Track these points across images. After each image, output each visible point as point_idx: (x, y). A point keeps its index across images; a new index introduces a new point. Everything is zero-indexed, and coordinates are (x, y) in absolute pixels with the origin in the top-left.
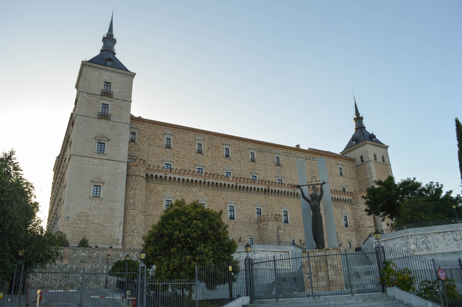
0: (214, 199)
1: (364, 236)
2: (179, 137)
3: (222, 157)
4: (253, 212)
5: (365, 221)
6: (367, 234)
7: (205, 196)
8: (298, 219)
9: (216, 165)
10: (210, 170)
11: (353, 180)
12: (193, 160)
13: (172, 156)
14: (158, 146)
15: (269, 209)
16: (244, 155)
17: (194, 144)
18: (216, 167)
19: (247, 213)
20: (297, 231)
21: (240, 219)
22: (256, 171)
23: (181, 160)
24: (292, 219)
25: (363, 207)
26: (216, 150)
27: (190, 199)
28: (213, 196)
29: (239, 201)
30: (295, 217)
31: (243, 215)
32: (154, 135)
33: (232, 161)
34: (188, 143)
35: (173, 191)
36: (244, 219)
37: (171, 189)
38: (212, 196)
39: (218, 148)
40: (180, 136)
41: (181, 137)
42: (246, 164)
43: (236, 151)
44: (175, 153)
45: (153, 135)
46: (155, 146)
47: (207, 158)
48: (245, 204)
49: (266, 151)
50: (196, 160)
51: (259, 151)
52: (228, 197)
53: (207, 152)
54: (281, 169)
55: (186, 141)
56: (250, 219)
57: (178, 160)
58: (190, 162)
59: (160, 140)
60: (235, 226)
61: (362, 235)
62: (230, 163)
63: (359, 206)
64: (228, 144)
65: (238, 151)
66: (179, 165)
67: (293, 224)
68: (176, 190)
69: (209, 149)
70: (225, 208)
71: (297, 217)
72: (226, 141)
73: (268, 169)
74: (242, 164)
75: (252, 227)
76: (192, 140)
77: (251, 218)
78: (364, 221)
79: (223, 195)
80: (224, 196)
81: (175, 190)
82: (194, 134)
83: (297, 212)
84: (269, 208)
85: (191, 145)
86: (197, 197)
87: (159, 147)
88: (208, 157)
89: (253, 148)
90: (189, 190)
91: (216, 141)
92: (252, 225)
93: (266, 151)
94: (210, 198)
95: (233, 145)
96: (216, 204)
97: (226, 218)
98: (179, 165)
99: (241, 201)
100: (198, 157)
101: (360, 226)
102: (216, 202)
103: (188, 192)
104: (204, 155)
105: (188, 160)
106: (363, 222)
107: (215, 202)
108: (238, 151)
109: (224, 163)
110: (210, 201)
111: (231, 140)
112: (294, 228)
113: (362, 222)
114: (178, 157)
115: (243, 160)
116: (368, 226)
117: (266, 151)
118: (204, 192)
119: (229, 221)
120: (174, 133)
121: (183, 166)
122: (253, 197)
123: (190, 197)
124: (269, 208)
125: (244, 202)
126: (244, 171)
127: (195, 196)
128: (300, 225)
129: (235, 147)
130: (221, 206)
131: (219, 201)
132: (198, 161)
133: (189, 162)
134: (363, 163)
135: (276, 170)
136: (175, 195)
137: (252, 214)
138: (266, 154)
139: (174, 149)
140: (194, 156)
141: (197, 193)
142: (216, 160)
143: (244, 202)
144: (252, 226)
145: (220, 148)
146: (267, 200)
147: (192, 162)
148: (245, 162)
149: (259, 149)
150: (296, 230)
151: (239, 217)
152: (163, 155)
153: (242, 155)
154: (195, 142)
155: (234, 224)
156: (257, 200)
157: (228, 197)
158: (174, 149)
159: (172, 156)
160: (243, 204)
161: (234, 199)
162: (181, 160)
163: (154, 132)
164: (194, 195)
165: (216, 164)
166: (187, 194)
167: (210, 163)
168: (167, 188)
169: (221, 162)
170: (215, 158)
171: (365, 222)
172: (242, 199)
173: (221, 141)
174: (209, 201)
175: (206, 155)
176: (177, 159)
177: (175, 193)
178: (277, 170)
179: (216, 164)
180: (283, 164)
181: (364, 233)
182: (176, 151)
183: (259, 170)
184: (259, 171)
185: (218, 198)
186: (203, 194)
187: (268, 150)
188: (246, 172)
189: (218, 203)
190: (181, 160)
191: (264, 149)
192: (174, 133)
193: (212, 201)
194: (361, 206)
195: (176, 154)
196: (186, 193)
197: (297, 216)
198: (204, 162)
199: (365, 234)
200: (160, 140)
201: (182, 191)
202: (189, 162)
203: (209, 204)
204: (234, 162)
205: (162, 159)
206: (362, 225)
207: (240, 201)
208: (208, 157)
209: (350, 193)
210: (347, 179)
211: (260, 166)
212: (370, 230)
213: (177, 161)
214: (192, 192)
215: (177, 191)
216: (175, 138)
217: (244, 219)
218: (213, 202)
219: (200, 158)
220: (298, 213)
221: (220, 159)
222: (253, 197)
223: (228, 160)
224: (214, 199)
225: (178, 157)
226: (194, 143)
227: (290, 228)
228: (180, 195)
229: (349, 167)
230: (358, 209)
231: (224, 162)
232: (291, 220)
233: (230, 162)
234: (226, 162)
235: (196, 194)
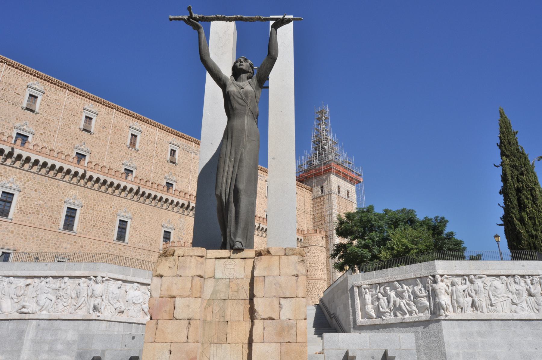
0: (95, 205)
1: (312, 291)
2: (54, 97)
3: (123, 144)
4: (158, 234)
5: (315, 271)
6: (316, 289)
7: (80, 197)
9: (112, 155)
10: (99, 159)
11: (307, 215)
12: (72, 139)
13: (34, 124)
14: (10, 101)
15: (184, 234)
16: (160, 150)
17: (79, 115)
18: (111, 158)
19: (148, 235)
21: (134, 243)
22: (175, 177)
23: (49, 134)
25: (316, 252)
26: (115, 133)
27: (51, 198)
28: (94, 200)
29: (138, 215)
31: (140, 237)
32: (7, 84)
33: (139, 154)
34: (69, 111)
35: (20, 178)
36: (141, 244)
37: (18, 175)
38: (93, 199)
39: (120, 130)
40: (57, 97)
41: (57, 99)
42: (161, 164)
43: (148, 141)
44: (42, 120)
45: (6, 83)
46: (5, 101)
47: (97, 140)
48: (147, 220)
49: (195, 151)
50: (76, 140)
51: (183, 150)
52: (122, 206)
53: (100, 132)
55: (66, 107)
56: (151, 244)
57: (44, 133)
58: (66, 140)
59: (18, 94)
60: (124, 253)
61: (309, 289)
62: (135, 156)
63: (310, 250)
64: (137, 128)
65: (152, 142)
66: (44, 141)
68: (27, 177)
69: (103, 128)
70: (113, 222)
72: (135, 123)
73: (193, 178)
74: (154, 161)
75: (153, 257)
76: (77, 107)
77: (153, 244)
78: (314, 270)
79: (113, 201)
80: (113, 204)
81: (25, 178)
82: (83, 101)
84: (185, 232)
85: (74, 116)
86: (65, 196)
87: (13, 104)
88: (100, 139)
89: (176, 144)
90: (52, 183)
91: (119, 120)
92: (153, 254)
93: (194, 152)
94: (89, 202)
95: (146, 132)
96: (98, 213)
97: (110, 237)
98: (44, 141)
99: (141, 215)
100: (82, 135)
101: (309, 276)
102: (98, 209)
103: (50, 186)
104: (94, 135)
105: (63, 137)
106: (313, 272)
107: (97, 209)
108: (152, 142)
109: (124, 154)
110: (87, 206)
111: (143, 124)
113: (312, 271)
114: (45, 127)
115: (156, 157)
116: (319, 277)
117: (194, 152)
118: (79, 191)
119: (114, 242)
120: (46, 90)
121: (51, 143)
122: (162, 213)
123: (52, 194)
124: (185, 232)
125: (147, 217)
126: (155, 172)
127: (62, 194)
129: (147, 135)
130: (105, 218)
131: (104, 210)
132: (81, 142)
133: (63, 140)
134: (323, 194)
136: (23, 185)
137: (156, 238)
138: (195, 156)
139: (41, 114)
140: (75, 133)
141: (67, 190)
142: (112, 147)
143: (147, 217)
144: (152, 255)
145: (123, 131)
146: (183, 220)
147: (69, 141)
148: (159, 160)
149: (185, 146)
151: (133, 240)
152: (17, 119)
153: (158, 149)
154: (81, 112)
155: (122, 249)
156: (168, 219)
157: (122, 206)
158: (41, 114)
159: (34, 124)
160: (144, 221)
161: (130, 210)
162: (50, 135)
163: (8, 78)
164: (61, 192)
165: (111, 153)
166: (47, 189)
167: (101, 149)
168: (10, 172)
169: (120, 151)
170: (111, 143)
171: (316, 272)
172: (144, 213)
173: (127, 121)
174: (86, 207)
175: (97, 136)
176: (42, 131)
177: (25, 183)
179: (111, 153)
181: (313, 287)
182: (44, 117)
183: (178, 176)
184: (179, 178)
185: (103, 205)
186: (78, 194)
187: (198, 151)
188: (158, 175)
189: (101, 211)
190: (50, 135)
191: (192, 149)
192: (46, 90)
193: (91, 207)
194: (313, 250)
195: (43, 123)
196: (45, 186)
198: (91, 145)
199: (314, 288)
200: (18, 94)
201: (40, 183)
202: (63, 140)
203: (85, 210)
204: (142, 156)
205: (13, 124)
206: (311, 275)
207: (140, 214)
208: (100, 139)
209: (301, 231)
210: (299, 212)
211: (182, 171)
212: (320, 283)
213: (41, 134)
214: (57, 187)
215: (28, 181)
216: (47, 97)
217: (141, 244)
218: (93, 210)
219: (84, 138)
221: (119, 147)
222: (162, 213)
223: (132, 152)
224: (95, 205)
225: (45, 127)
226: (79, 112)
228: (33, 187)
229: (304, 197)
230: (308, 254)
231: (126, 154)
233: (136, 154)
234: (129, 154)
235: (64, 191)
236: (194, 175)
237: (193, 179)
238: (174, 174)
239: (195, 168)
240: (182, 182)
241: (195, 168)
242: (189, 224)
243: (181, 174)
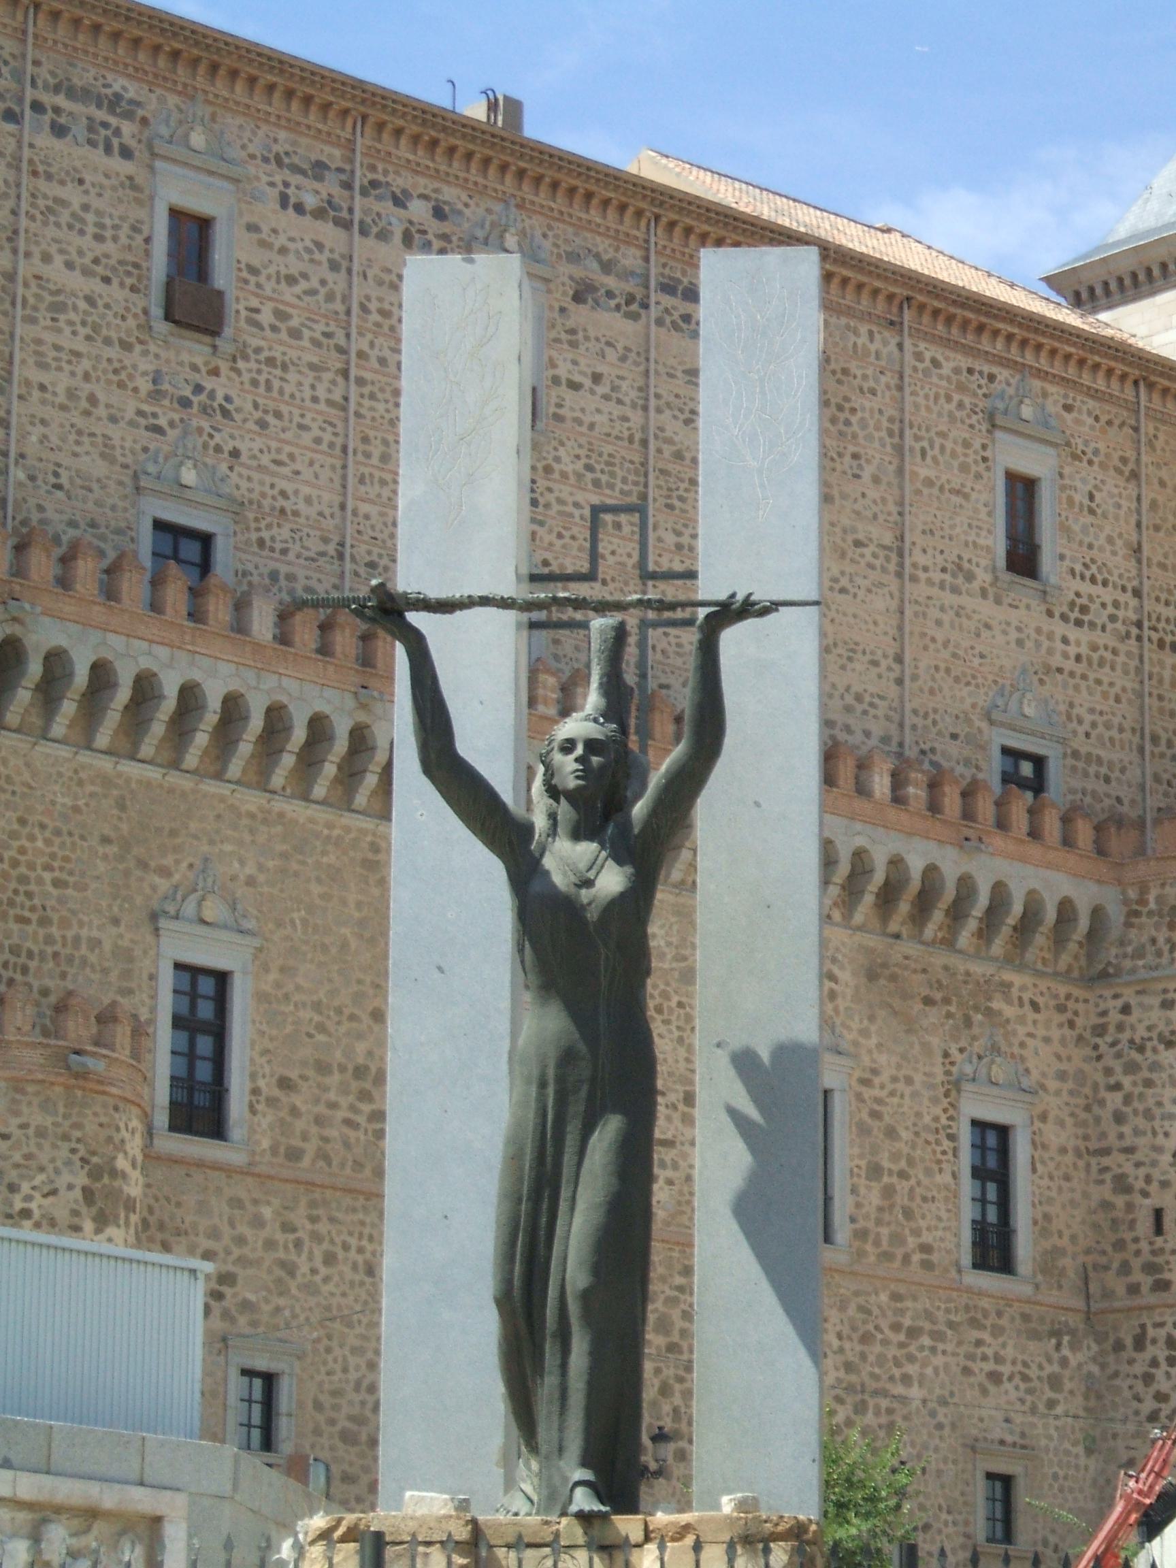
20: (330, 1259)
24: (285, 1084)
30: (323, 1068)
54: (220, 387)
67: (294, 1155)
112: (299, 1217)
135: (145, 385)
150: (317, 1237)
178: (156, 395)
180: (266, 317)
227: (236, 1203)
232: (272, 1102)
236: (49, 337)
239: (58, 260)
241: (58, 260)
242: (22, 821)
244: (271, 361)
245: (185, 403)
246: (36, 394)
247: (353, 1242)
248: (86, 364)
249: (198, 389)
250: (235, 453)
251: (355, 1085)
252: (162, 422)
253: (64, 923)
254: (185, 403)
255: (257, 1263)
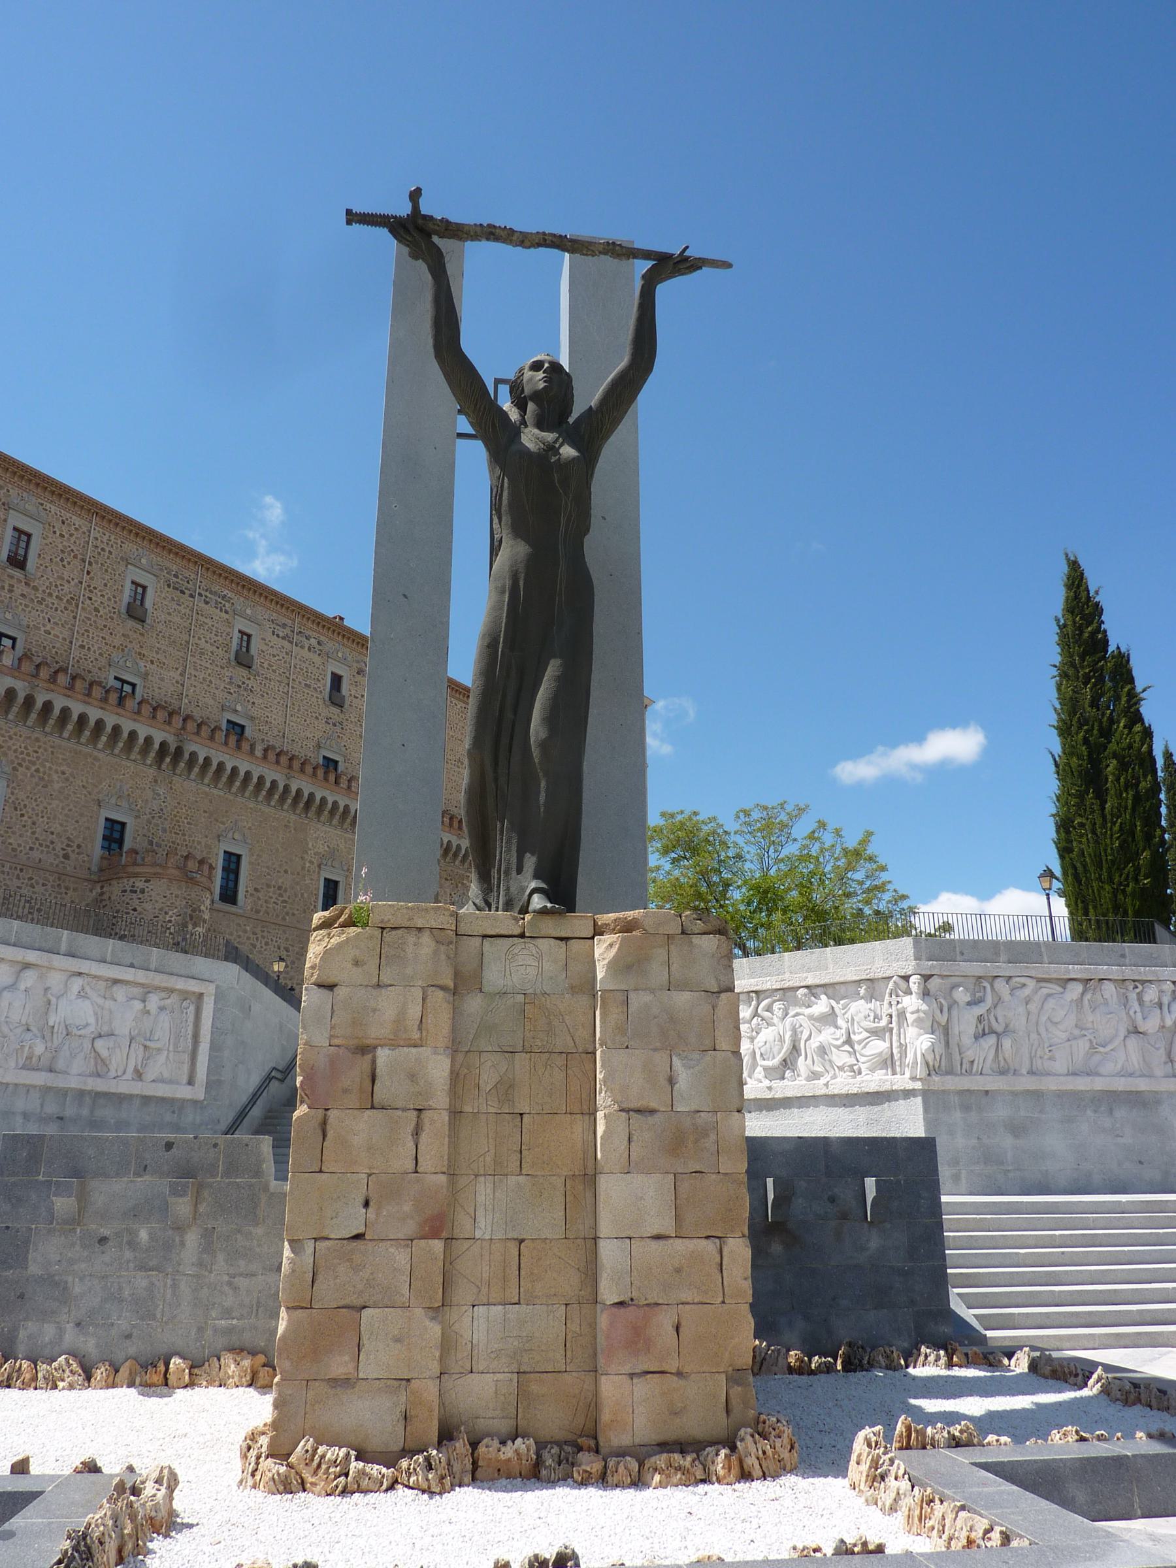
8: (280, 895)
20: (267, 944)
24: (256, 890)
30: (268, 886)
54: (250, 683)
67: (258, 912)
71: (280, 888)
83: (281, 866)
112: (258, 930)
128: (284, 919)
135: (227, 680)
150: (263, 937)
178: (231, 683)
180: (266, 665)
184: (153, 667)
197: (280, 881)
220: (286, 872)
227: (239, 925)
232: (252, 895)
237: (193, 673)
238: (140, 654)
239: (203, 640)
240: (162, 679)
241: (203, 640)
243: (159, 656)
244: (266, 678)
245: (239, 686)
246: (193, 678)
247: (274, 939)
248: (210, 671)
249: (244, 683)
250: (253, 703)
251: (278, 892)
252: (232, 691)
253: (190, 836)
254: (239, 686)
255: (244, 944)
